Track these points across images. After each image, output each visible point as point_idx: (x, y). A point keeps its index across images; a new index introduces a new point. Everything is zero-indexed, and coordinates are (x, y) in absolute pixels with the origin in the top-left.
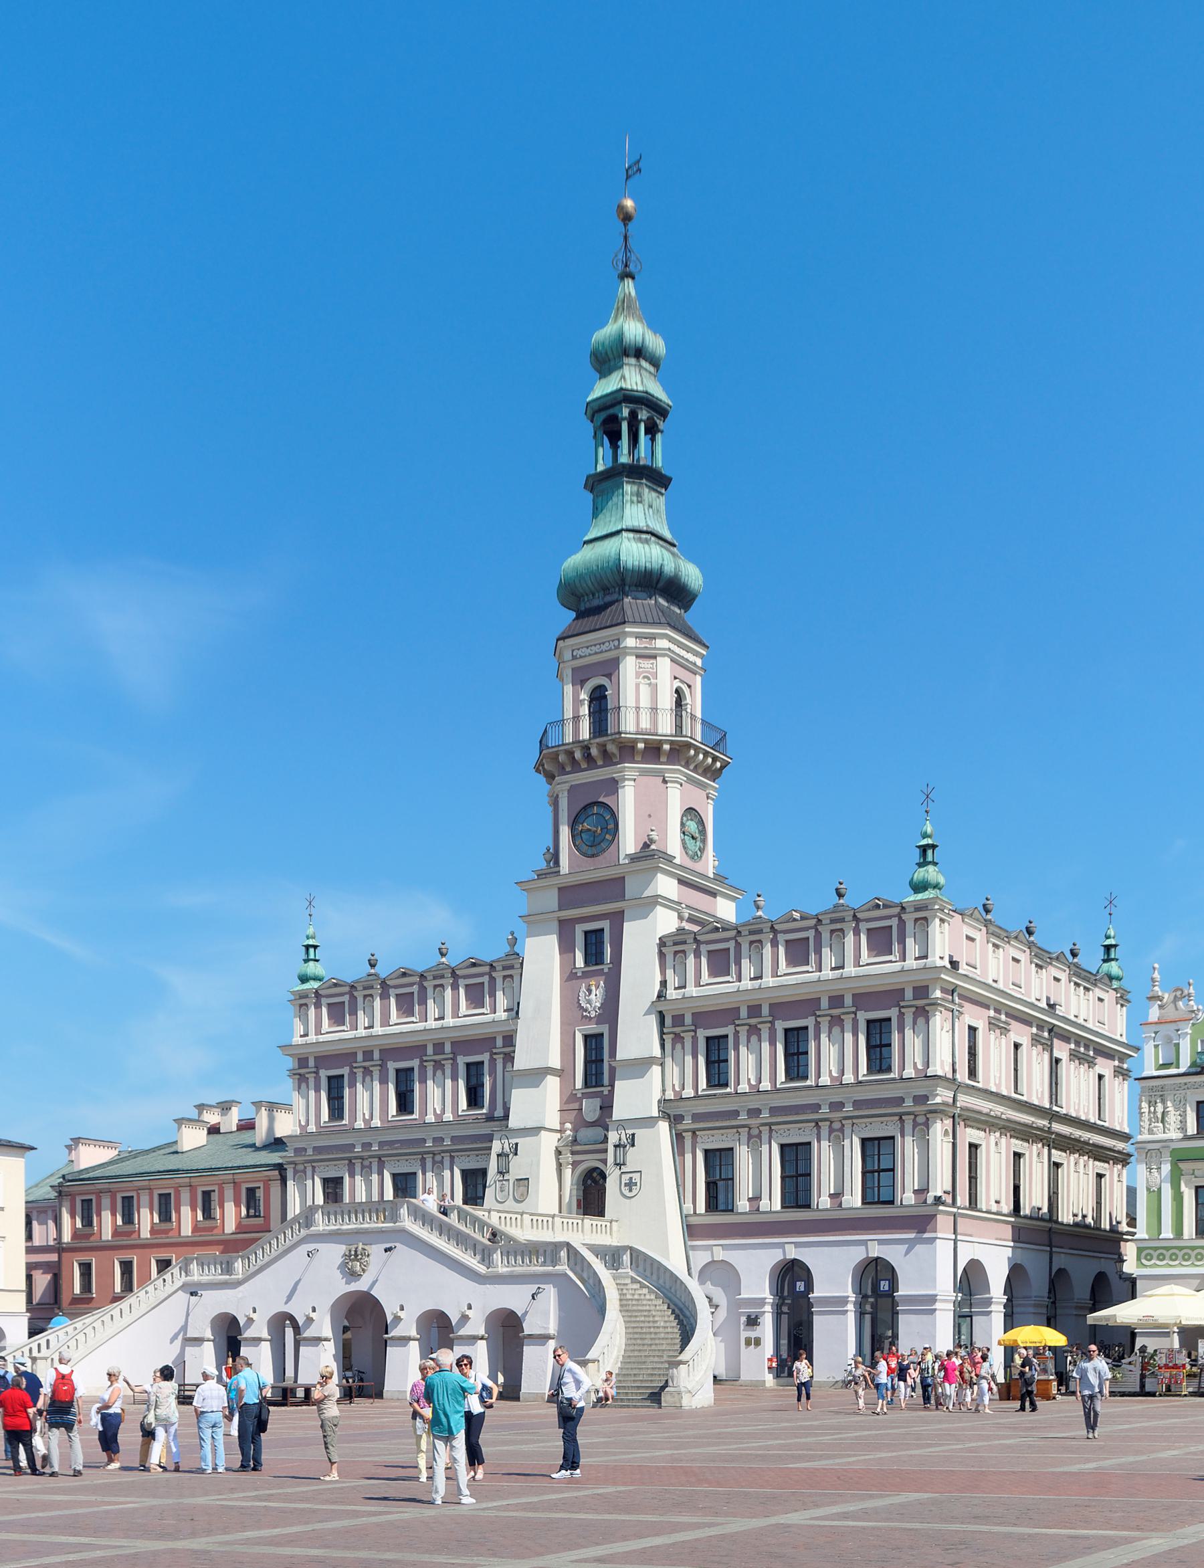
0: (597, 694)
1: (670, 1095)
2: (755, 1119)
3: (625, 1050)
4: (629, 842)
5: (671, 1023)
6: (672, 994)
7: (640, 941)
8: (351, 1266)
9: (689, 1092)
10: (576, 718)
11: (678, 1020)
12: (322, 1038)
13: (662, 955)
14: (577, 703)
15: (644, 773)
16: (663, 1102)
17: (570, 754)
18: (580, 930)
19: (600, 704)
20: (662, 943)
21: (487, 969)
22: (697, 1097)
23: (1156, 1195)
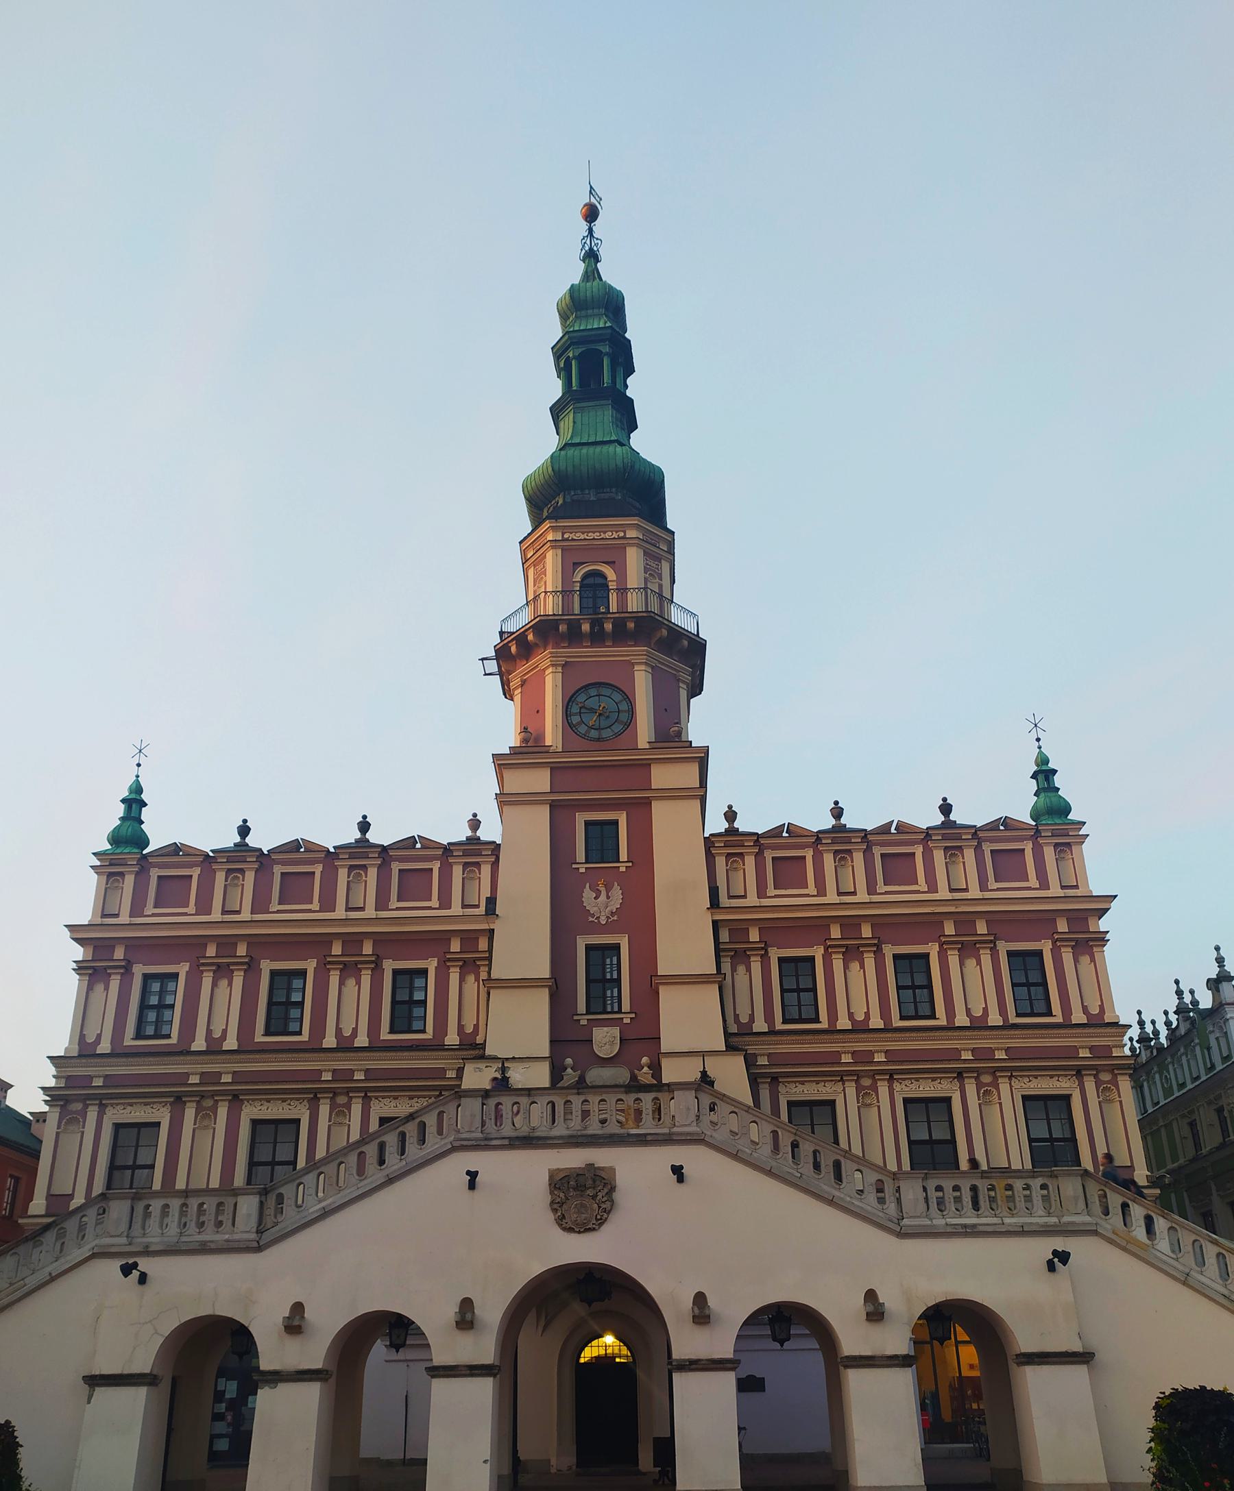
0: (590, 581)
1: (733, 1029)
6: (724, 901)
8: (582, 1199)
11: (739, 930)
16: (727, 1035)
17: (574, 626)
18: (581, 819)
21: (440, 852)
22: (772, 1032)
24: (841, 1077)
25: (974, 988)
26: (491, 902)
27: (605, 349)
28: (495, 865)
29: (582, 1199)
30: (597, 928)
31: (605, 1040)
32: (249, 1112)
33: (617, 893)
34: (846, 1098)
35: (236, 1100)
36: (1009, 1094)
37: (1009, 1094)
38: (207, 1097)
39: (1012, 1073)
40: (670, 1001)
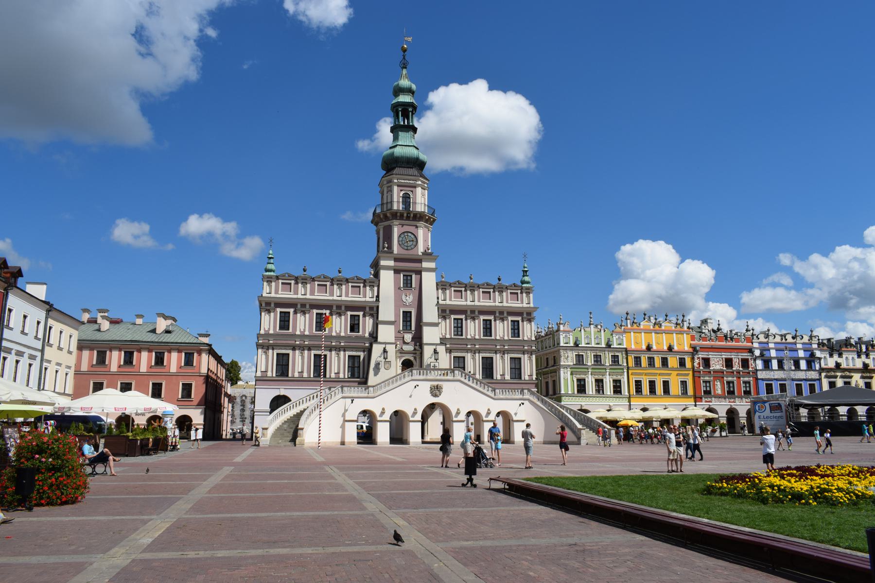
2: (473, 347)
3: (426, 318)
4: (421, 249)
5: (444, 312)
6: (441, 302)
7: (429, 281)
8: (436, 391)
9: (271, 332)
10: (398, 202)
11: (444, 311)
12: (278, 296)
13: (437, 289)
14: (398, 198)
15: (426, 227)
19: (406, 198)
20: (437, 284)
23: (566, 380)
24: (467, 351)
25: (501, 330)
26: (378, 296)
27: (410, 109)
28: (378, 286)
29: (436, 391)
30: (406, 306)
31: (408, 337)
32: (313, 352)
33: (411, 297)
34: (468, 356)
35: (309, 349)
36: (507, 357)
37: (507, 357)
38: (302, 348)
39: (508, 351)
40: (426, 330)
